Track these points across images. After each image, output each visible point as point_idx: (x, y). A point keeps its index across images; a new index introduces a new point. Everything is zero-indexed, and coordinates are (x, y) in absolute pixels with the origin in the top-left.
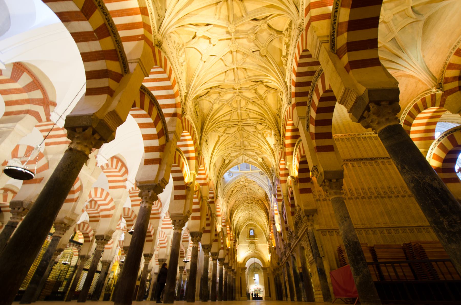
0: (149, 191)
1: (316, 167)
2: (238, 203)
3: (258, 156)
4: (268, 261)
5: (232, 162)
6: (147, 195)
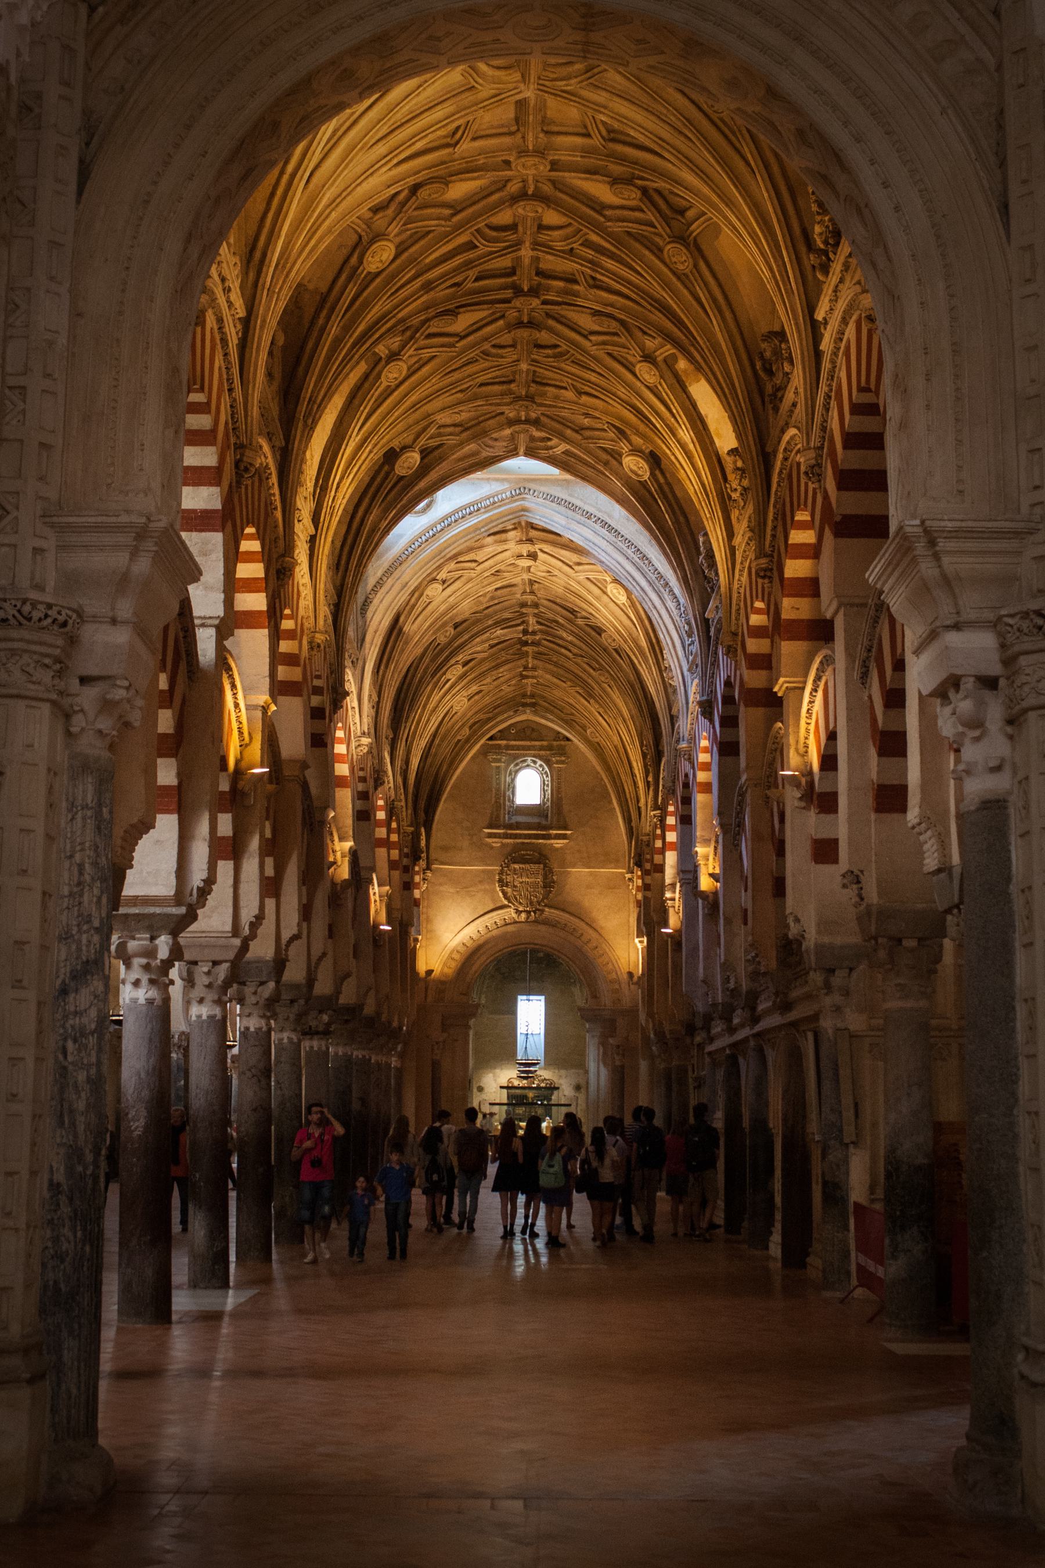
0: (155, 934)
1: (857, 876)
2: (450, 643)
3: (625, 447)
4: (630, 974)
5: (441, 459)
6: (150, 953)
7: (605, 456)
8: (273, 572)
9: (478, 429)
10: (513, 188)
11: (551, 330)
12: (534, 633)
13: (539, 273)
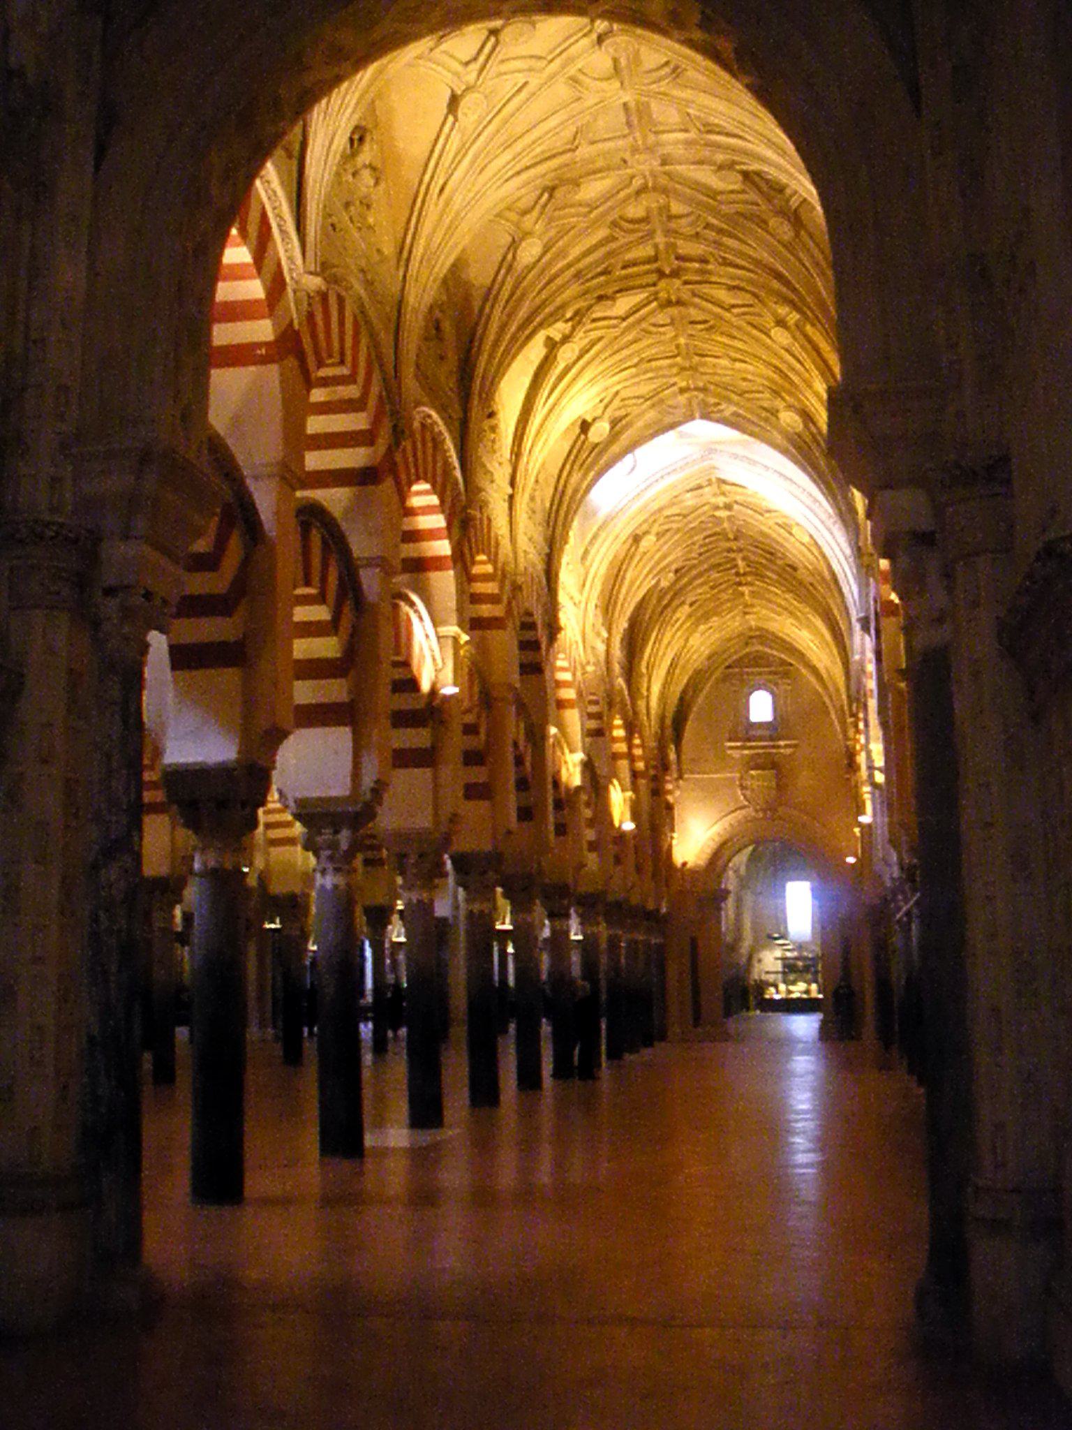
3: (779, 404)
7: (764, 414)
8: (456, 523)
9: (655, 399)
10: (637, 183)
11: (696, 306)
12: (745, 574)
13: (679, 258)
